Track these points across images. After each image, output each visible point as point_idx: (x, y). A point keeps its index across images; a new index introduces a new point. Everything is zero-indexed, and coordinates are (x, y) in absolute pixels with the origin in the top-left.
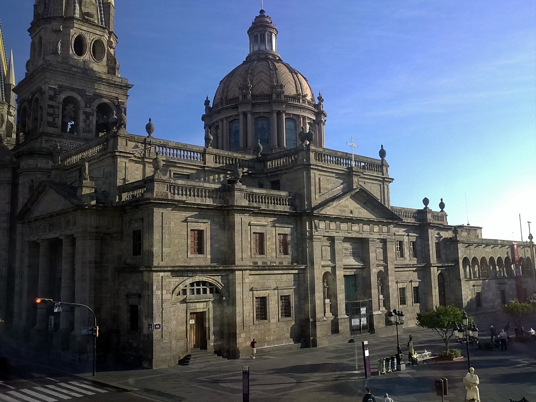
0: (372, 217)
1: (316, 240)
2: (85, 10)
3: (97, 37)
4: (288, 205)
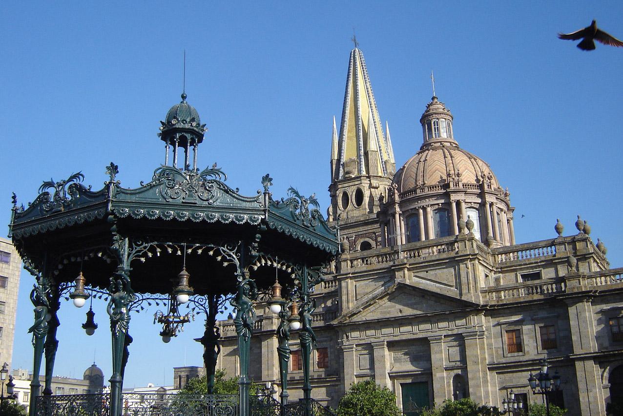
0: (408, 311)
1: (346, 350)
2: (347, 169)
3: (355, 188)
4: (323, 320)
